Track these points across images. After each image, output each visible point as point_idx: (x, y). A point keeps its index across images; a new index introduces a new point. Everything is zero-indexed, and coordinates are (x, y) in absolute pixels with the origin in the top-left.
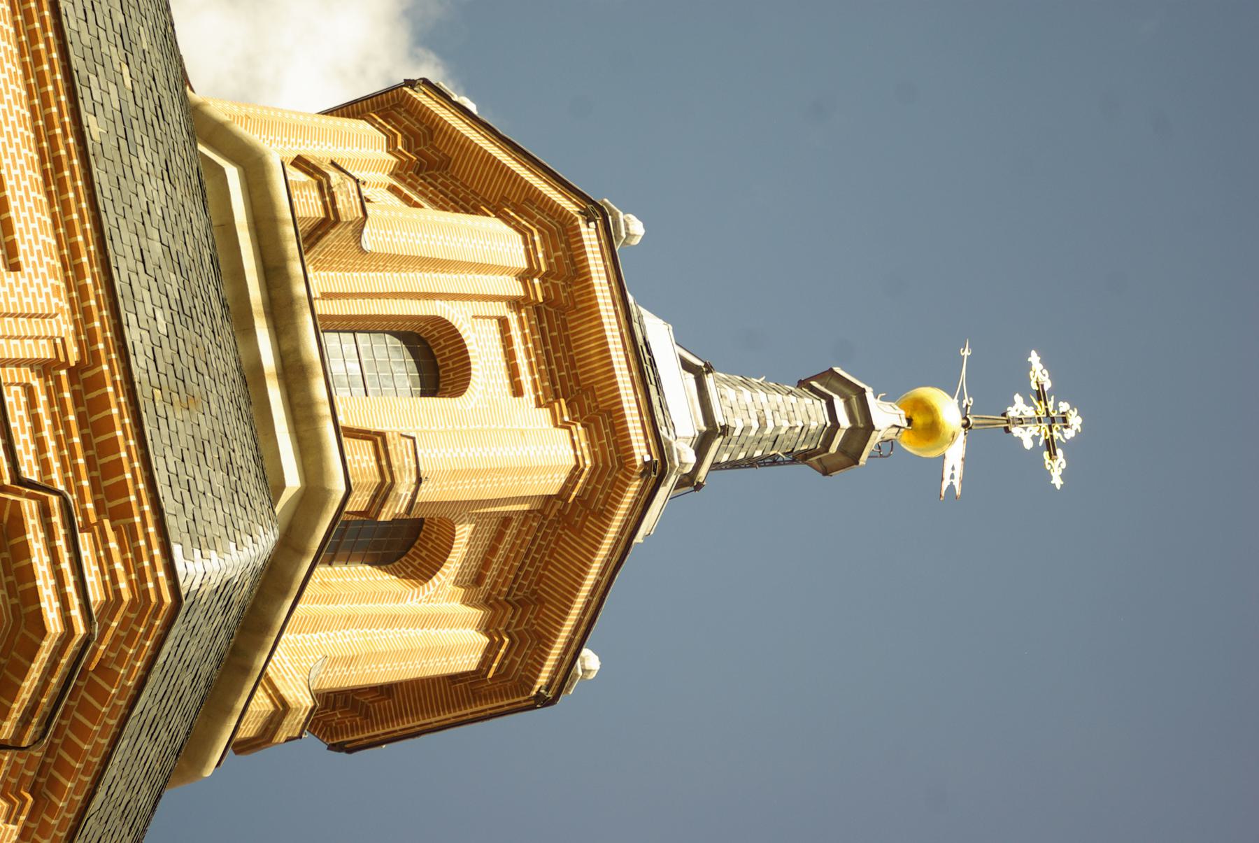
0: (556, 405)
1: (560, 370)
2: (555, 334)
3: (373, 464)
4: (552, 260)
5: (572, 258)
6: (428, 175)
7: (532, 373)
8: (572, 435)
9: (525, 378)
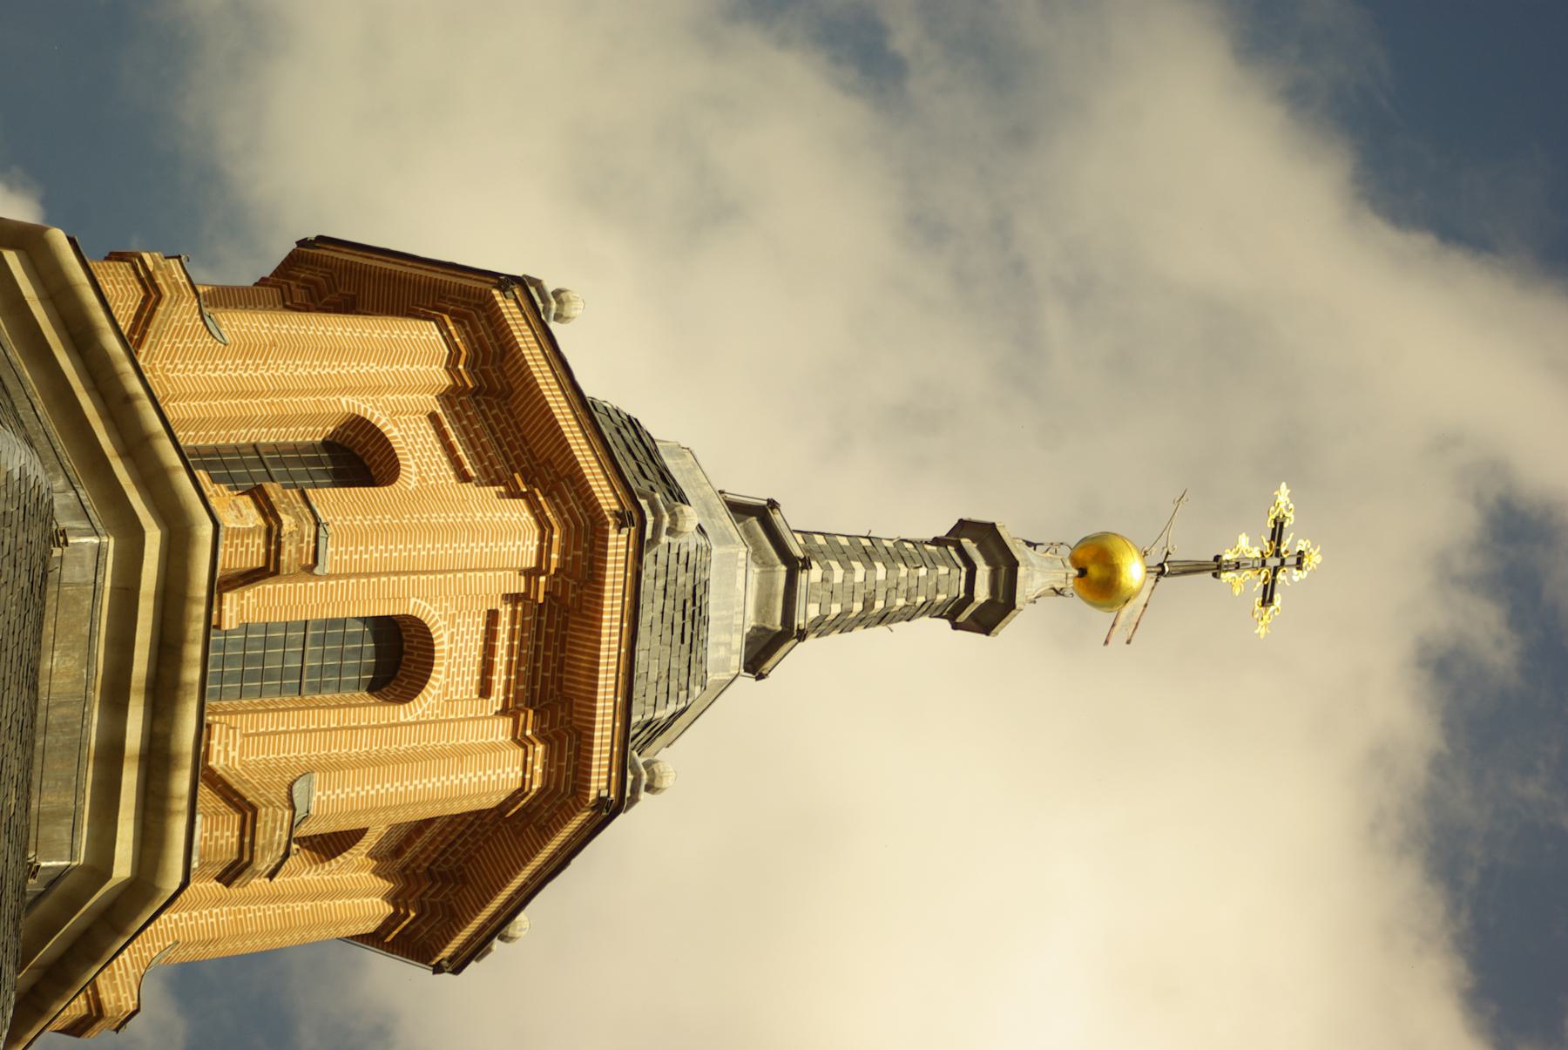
0: (522, 716)
1: (545, 669)
2: (551, 631)
4: (569, 558)
5: (592, 561)
6: (484, 400)
7: (509, 672)
8: (526, 755)
9: (499, 678)
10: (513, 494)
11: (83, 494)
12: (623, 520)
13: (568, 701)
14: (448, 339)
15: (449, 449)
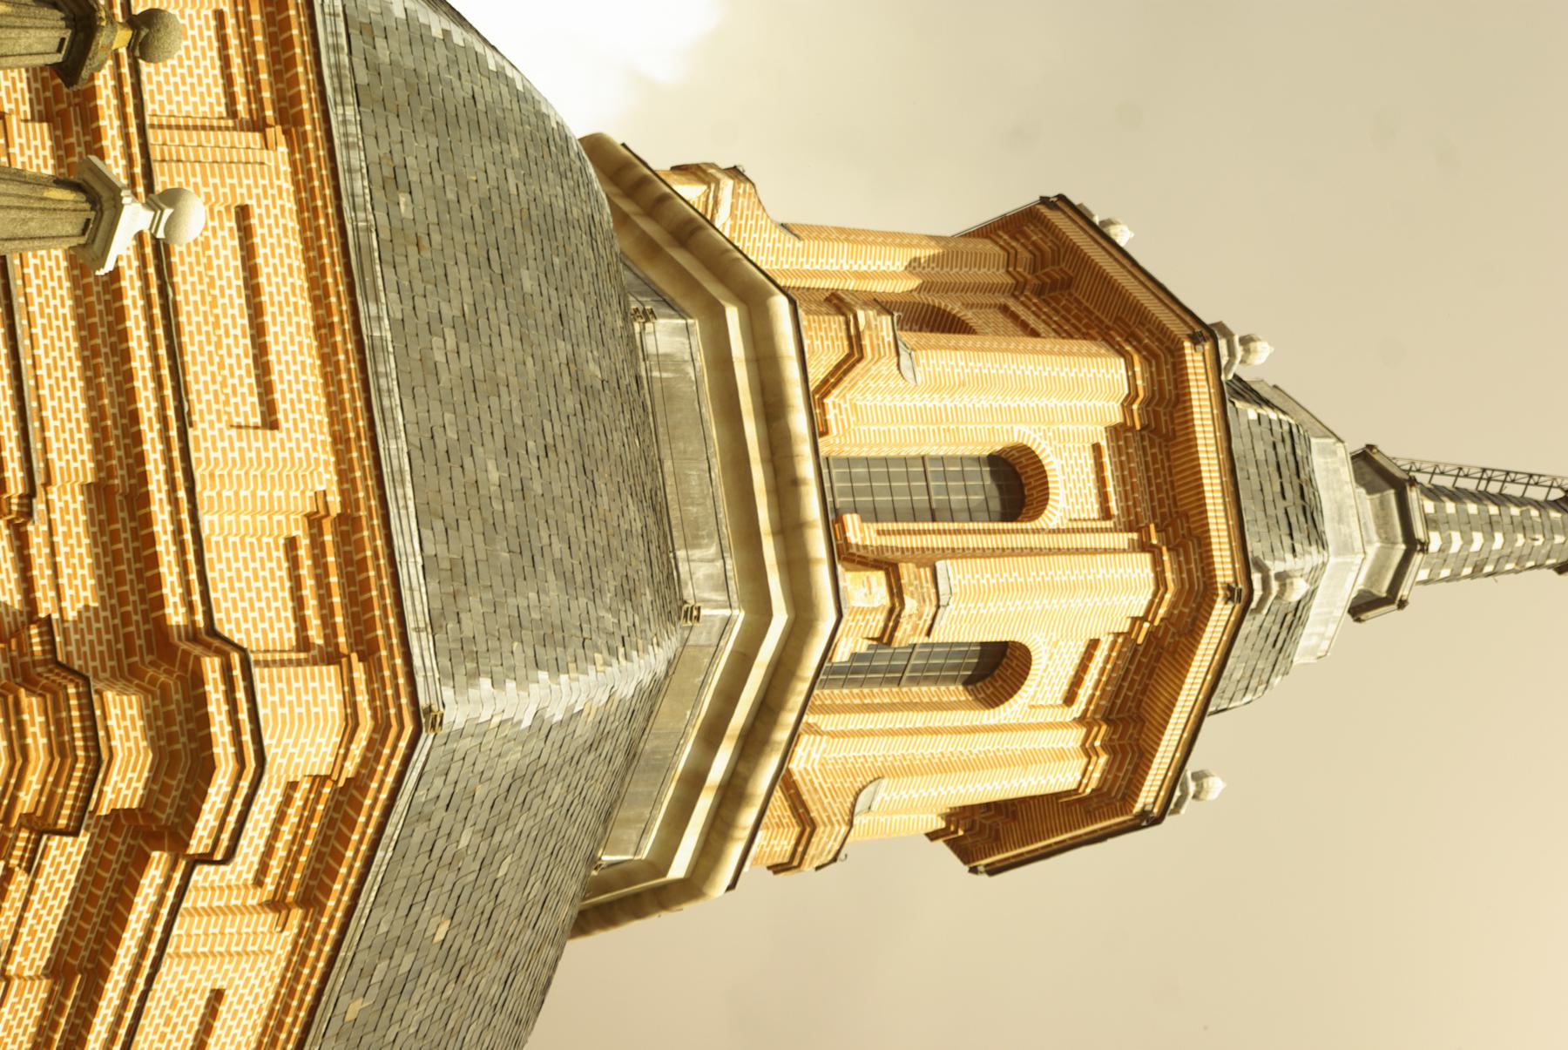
0: (1096, 729)
1: (1130, 689)
2: (1144, 660)
3: (789, 848)
4: (1176, 612)
5: (1195, 620)
7: (1096, 688)
8: (1088, 764)
10: (1144, 546)
11: (730, 564)
12: (1231, 594)
13: (1140, 721)
14: (1132, 379)
15: (1101, 482)
